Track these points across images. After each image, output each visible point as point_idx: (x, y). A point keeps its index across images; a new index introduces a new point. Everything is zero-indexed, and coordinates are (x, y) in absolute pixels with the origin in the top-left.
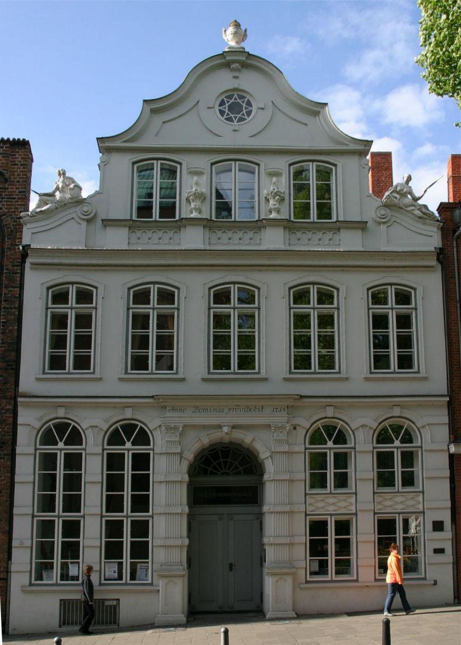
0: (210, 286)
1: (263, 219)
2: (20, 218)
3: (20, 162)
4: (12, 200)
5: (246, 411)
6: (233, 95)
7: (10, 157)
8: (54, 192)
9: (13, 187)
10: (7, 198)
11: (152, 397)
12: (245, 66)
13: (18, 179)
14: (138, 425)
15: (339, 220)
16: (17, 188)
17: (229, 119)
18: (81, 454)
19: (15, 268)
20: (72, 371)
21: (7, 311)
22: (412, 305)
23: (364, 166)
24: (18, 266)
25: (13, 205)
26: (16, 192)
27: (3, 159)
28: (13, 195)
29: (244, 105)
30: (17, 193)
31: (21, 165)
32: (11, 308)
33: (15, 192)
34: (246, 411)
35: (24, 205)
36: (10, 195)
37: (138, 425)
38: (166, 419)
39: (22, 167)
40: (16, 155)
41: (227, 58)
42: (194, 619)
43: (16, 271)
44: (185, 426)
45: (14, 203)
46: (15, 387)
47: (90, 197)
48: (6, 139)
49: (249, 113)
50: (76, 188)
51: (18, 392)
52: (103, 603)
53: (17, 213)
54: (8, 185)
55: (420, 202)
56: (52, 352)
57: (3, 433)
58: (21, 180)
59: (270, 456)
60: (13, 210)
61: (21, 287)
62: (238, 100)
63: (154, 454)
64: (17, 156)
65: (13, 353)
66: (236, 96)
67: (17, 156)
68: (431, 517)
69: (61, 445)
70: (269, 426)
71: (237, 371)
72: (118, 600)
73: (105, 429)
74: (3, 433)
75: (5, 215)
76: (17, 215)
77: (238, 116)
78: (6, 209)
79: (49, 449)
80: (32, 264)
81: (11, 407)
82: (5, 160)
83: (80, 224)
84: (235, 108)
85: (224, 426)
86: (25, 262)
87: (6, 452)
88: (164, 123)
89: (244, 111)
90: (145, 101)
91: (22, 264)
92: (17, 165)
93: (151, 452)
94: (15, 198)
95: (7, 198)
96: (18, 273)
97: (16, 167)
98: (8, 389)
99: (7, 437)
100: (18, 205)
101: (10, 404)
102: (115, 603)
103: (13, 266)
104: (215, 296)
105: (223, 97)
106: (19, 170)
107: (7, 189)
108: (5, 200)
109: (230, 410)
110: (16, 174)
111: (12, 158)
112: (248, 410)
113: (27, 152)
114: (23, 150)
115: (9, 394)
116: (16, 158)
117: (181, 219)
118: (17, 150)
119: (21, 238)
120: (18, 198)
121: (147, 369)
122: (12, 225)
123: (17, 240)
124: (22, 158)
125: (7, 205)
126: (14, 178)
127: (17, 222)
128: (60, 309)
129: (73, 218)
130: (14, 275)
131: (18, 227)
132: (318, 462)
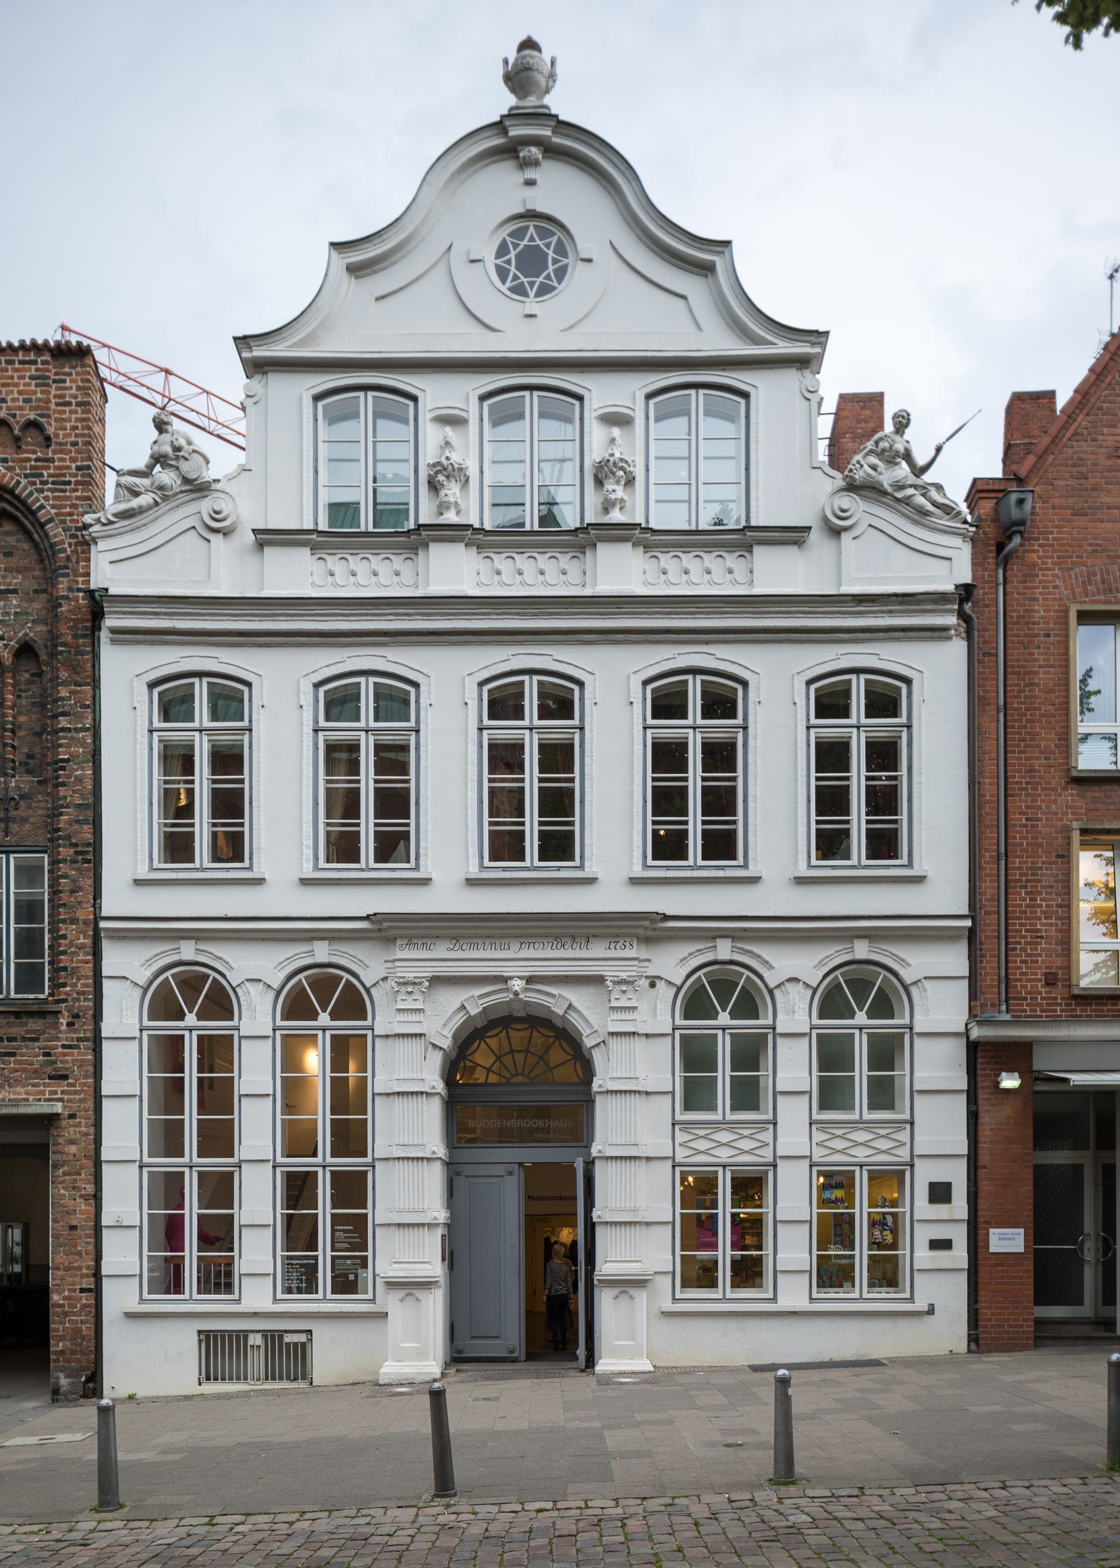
0: (481, 679)
1: (588, 525)
2: (86, 527)
3: (75, 397)
4: (63, 487)
5: (554, 947)
6: (527, 228)
7: (54, 386)
8: (151, 467)
9: (64, 456)
10: (54, 483)
12: (553, 152)
13: (73, 439)
14: (342, 978)
15: (753, 523)
17: (519, 290)
18: (232, 1036)
19: (81, 641)
20: (207, 864)
21: (69, 735)
22: (901, 717)
23: (808, 395)
24: (84, 636)
27: (38, 389)
28: (64, 475)
29: (551, 253)
30: (74, 471)
32: (77, 730)
33: (68, 468)
34: (554, 947)
35: (89, 499)
36: (58, 475)
37: (342, 978)
38: (397, 964)
39: (79, 409)
40: (64, 381)
41: (511, 134)
42: (458, 1371)
43: (82, 648)
45: (68, 494)
46: (95, 899)
47: (231, 478)
48: (40, 341)
49: (561, 273)
52: (281, 1338)
53: (75, 517)
54: (54, 452)
55: (928, 477)
57: (75, 995)
58: (80, 440)
59: (603, 1042)
60: (68, 510)
61: (96, 683)
62: (538, 242)
63: (374, 1037)
64: (68, 384)
65: (87, 828)
66: (532, 230)
67: (68, 384)
68: (925, 1174)
69: (191, 1019)
70: (599, 980)
72: (310, 1332)
73: (276, 985)
74: (75, 995)
75: (51, 520)
76: (77, 521)
78: (52, 508)
79: (168, 1027)
80: (114, 631)
83: (209, 541)
84: (532, 261)
85: (511, 978)
86: (100, 629)
87: (82, 1035)
89: (551, 268)
90: (333, 244)
91: (93, 633)
92: (69, 404)
93: (369, 1033)
94: (69, 483)
95: (54, 483)
96: (86, 653)
97: (67, 409)
99: (82, 1003)
100: (77, 498)
102: (303, 1338)
103: (75, 636)
104: (491, 704)
105: (504, 233)
106: (74, 416)
107: (53, 461)
108: (50, 486)
109: (523, 945)
110: (68, 425)
112: (559, 947)
113: (89, 373)
114: (79, 369)
116: (66, 388)
117: (420, 527)
118: (67, 370)
119: (88, 575)
120: (77, 483)
121: (358, 861)
122: (66, 545)
124: (79, 388)
125: (55, 498)
127: (76, 536)
128: (177, 732)
129: (194, 527)
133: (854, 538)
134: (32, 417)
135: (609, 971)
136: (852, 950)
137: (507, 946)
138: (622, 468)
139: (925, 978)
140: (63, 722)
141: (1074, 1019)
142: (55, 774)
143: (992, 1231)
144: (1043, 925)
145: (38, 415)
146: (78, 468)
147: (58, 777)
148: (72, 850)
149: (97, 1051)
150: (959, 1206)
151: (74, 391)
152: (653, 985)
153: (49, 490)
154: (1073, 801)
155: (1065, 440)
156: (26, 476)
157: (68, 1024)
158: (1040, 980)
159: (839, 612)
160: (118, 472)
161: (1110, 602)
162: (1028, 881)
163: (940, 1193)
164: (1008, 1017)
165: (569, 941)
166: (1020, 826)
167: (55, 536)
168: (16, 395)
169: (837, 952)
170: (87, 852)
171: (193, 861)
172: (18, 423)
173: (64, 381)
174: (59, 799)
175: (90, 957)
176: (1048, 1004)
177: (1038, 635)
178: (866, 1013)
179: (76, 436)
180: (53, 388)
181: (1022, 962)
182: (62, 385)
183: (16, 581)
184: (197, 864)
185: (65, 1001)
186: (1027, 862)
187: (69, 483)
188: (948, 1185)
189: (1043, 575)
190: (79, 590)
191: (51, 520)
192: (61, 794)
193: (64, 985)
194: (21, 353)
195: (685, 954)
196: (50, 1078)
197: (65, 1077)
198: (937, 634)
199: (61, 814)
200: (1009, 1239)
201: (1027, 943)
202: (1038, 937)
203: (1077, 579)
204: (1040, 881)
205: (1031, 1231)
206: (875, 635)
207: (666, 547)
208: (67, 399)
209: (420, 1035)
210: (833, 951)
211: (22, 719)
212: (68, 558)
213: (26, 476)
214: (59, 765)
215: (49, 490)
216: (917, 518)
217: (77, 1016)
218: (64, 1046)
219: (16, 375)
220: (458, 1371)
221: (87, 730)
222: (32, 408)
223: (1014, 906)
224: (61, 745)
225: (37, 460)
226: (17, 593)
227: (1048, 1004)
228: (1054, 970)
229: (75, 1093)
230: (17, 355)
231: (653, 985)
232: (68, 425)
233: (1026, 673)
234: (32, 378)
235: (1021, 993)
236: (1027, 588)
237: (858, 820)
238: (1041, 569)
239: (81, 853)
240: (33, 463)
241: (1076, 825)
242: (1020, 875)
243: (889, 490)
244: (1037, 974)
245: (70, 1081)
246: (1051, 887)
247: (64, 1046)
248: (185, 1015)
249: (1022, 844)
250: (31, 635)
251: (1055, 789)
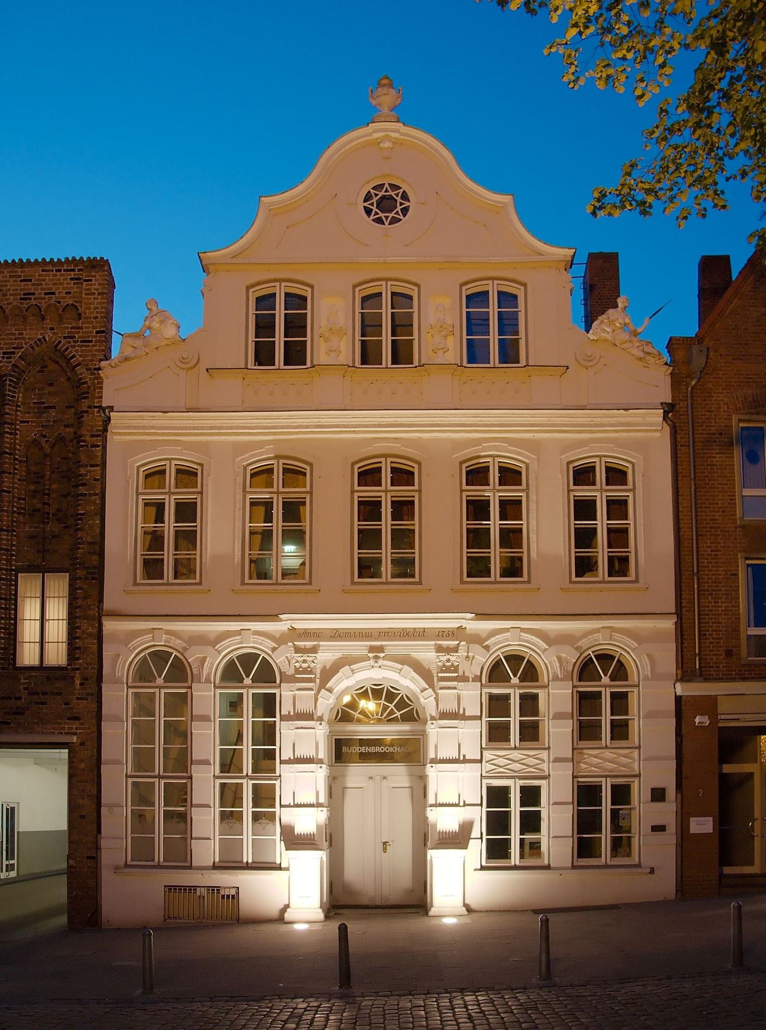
3: (98, 290)
7: (85, 283)
16: (94, 327)
25: (90, 351)
26: (93, 332)
31: (99, 294)
36: (85, 337)
40: (91, 280)
43: (95, 443)
49: (405, 211)
51: (103, 609)
53: (94, 362)
56: (143, 555)
57: (85, 666)
60: (90, 358)
65: (95, 557)
71: (390, 579)
75: (79, 364)
81: (95, 631)
82: (77, 288)
92: (94, 294)
94: (91, 341)
96: (98, 446)
97: (93, 297)
98: (89, 606)
100: (96, 350)
101: (92, 626)
107: (82, 328)
108: (79, 343)
110: (92, 307)
111: (86, 285)
115: (90, 613)
118: (93, 274)
120: (96, 341)
122: (88, 380)
123: (96, 401)
126: (90, 313)
127: (95, 374)
130: (94, 449)
131: (96, 381)
132: (498, 705)
134: (71, 302)
137: (370, 635)
140: (82, 490)
142: (76, 522)
145: (75, 301)
146: (97, 332)
147: (78, 524)
148: (85, 572)
151: (97, 286)
153: (79, 346)
156: (65, 338)
160: (123, 335)
162: (713, 590)
163: (658, 795)
166: (708, 555)
167: (81, 374)
168: (61, 290)
170: (95, 573)
171: (163, 578)
172: (61, 306)
173: (91, 280)
174: (79, 539)
175: (96, 641)
178: (610, 677)
179: (97, 313)
180: (84, 285)
182: (90, 283)
183: (53, 401)
184: (165, 581)
185: (78, 669)
187: (91, 341)
189: (717, 397)
190: (95, 407)
191: (79, 364)
192: (79, 536)
193: (78, 659)
194: (65, 265)
196: (69, 719)
197: (77, 719)
199: (79, 548)
205: (717, 818)
208: (92, 291)
211: (54, 486)
212: (89, 387)
213: (65, 338)
214: (79, 517)
215: (79, 346)
217: (86, 679)
218: (77, 699)
219: (62, 278)
220: (336, 914)
221: (97, 494)
222: (71, 298)
223: (704, 607)
224: (79, 505)
225: (71, 328)
226: (55, 408)
229: (84, 729)
230: (63, 266)
232: (92, 307)
233: (708, 458)
234: (71, 279)
236: (708, 405)
237: (602, 551)
238: (714, 393)
239: (91, 573)
240: (69, 330)
242: (708, 586)
245: (81, 721)
247: (77, 699)
248: (156, 678)
250: (63, 434)
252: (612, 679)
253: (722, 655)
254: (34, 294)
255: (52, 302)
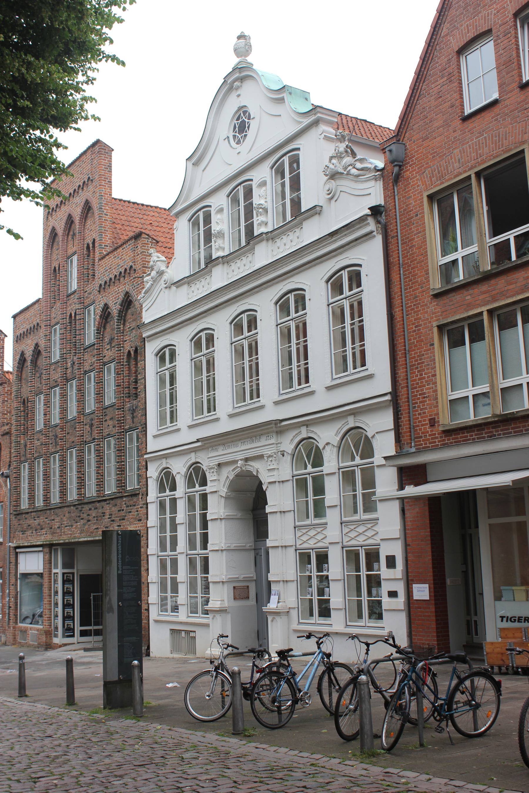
11: (198, 441)
44: (219, 465)
50: (158, 263)
77: (243, 134)
88: (203, 171)
133: (336, 201)
135: (267, 451)
136: (347, 423)
138: (261, 208)
139: (377, 433)
141: (445, 446)
143: (414, 585)
144: (427, 389)
149: (147, 508)
150: (399, 570)
152: (283, 455)
154: (435, 309)
155: (415, 102)
157: (142, 498)
158: (426, 424)
159: (327, 244)
161: (443, 183)
162: (419, 364)
163: (391, 562)
164: (413, 450)
165: (254, 438)
169: (343, 425)
176: (432, 439)
177: (412, 217)
181: (419, 414)
186: (417, 353)
188: (393, 557)
189: (412, 182)
195: (291, 437)
198: (368, 237)
200: (422, 591)
201: (421, 402)
202: (424, 397)
203: (427, 176)
204: (423, 363)
206: (345, 248)
207: (279, 236)
209: (216, 492)
210: (341, 425)
216: (355, 179)
227: (432, 439)
228: (433, 417)
231: (283, 455)
233: (409, 241)
235: (419, 433)
241: (435, 324)
243: (342, 171)
244: (425, 421)
246: (428, 365)
249: (414, 342)
251: (426, 305)
252: (362, 458)
253: (426, 424)
254: (120, 265)
255: (126, 267)
